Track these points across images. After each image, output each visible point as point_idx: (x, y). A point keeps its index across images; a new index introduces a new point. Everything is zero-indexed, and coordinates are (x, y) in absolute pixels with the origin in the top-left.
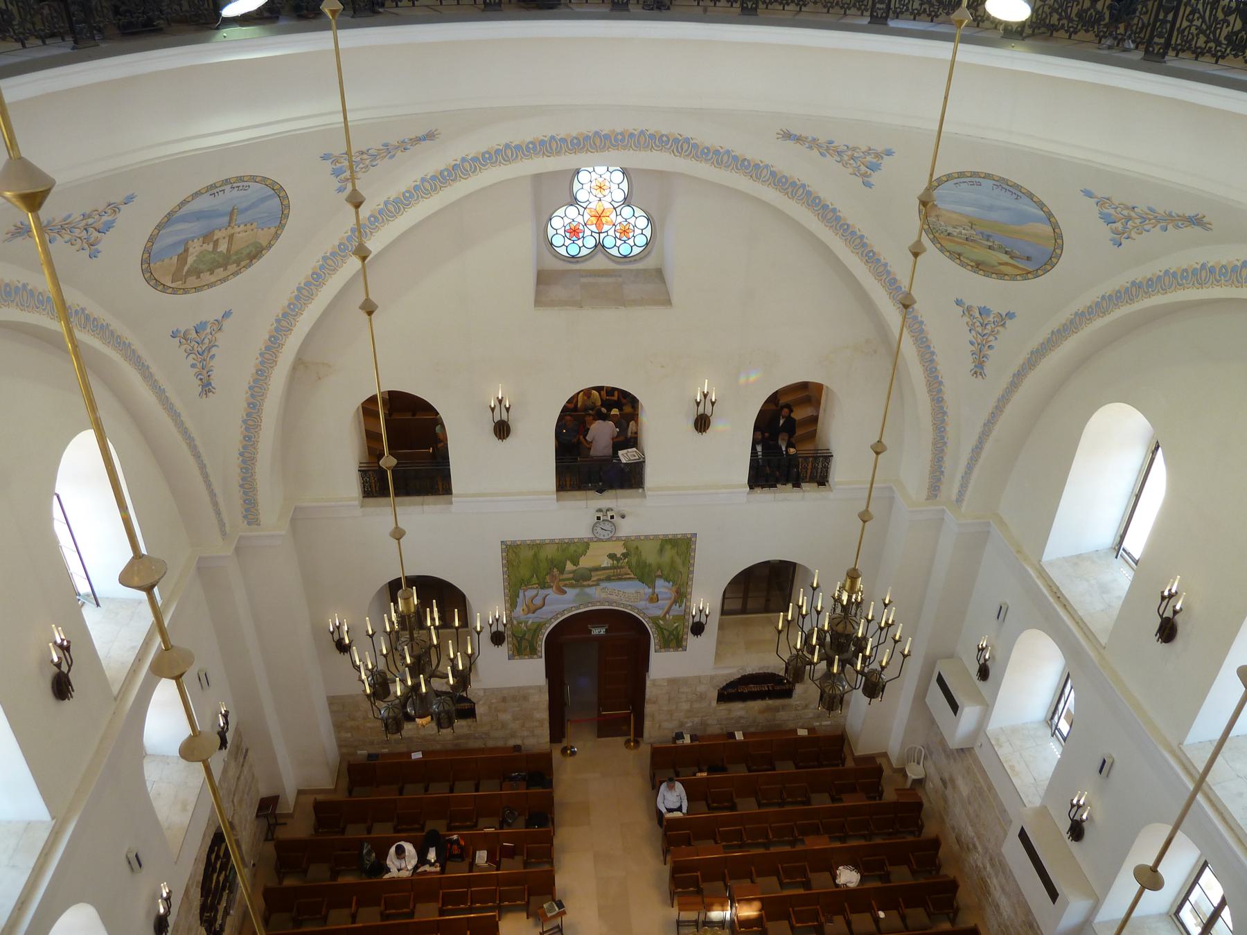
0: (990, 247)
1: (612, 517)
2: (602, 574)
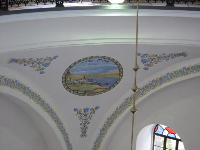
0: (91, 84)
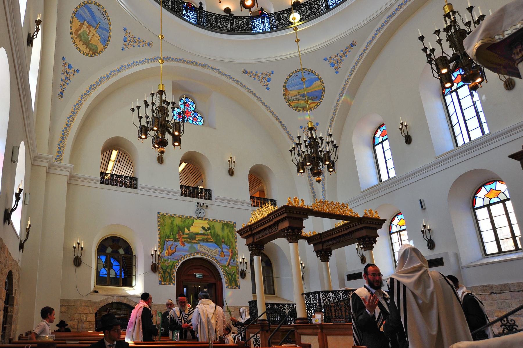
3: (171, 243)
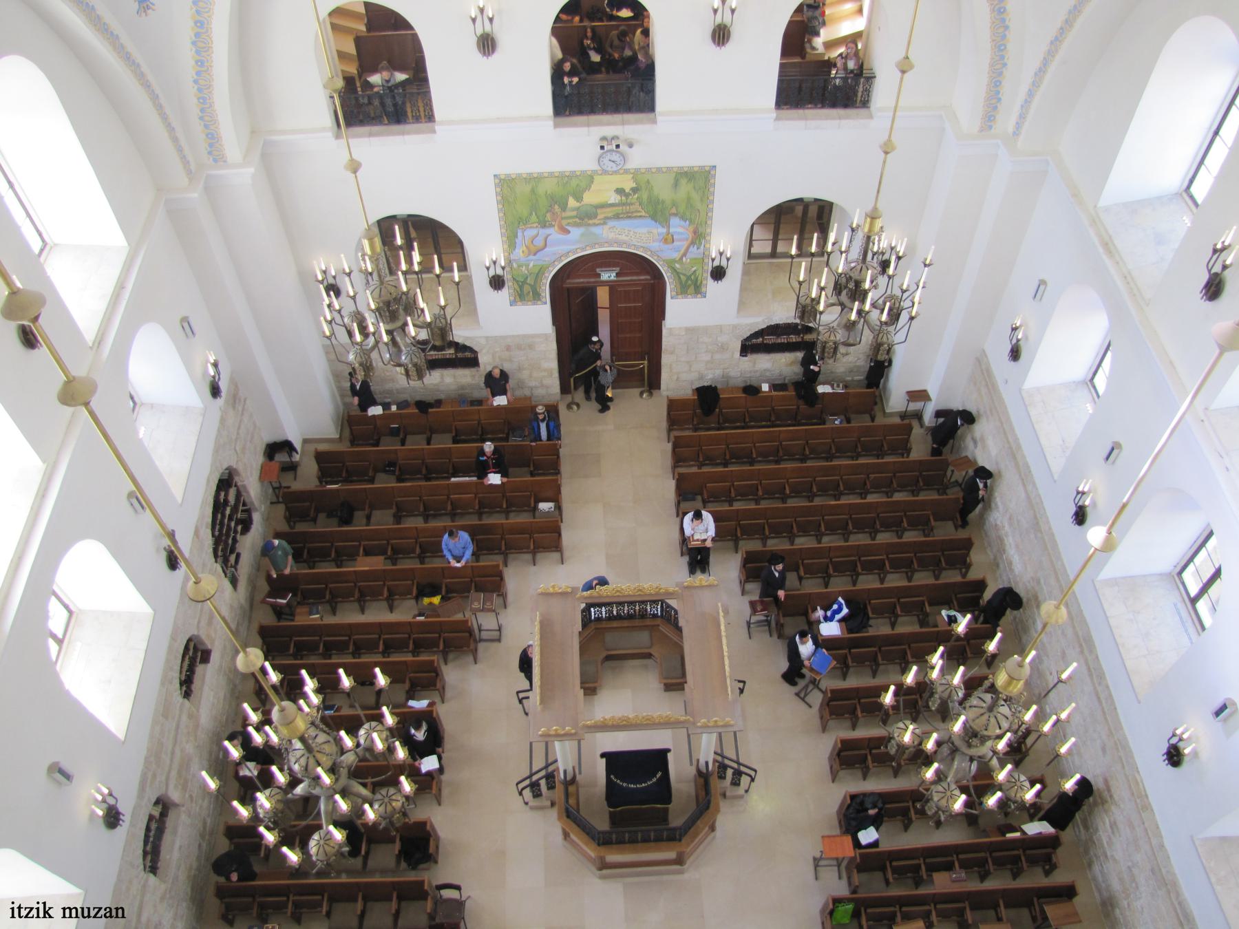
1: (618, 146)
2: (609, 212)
3: (534, 232)
